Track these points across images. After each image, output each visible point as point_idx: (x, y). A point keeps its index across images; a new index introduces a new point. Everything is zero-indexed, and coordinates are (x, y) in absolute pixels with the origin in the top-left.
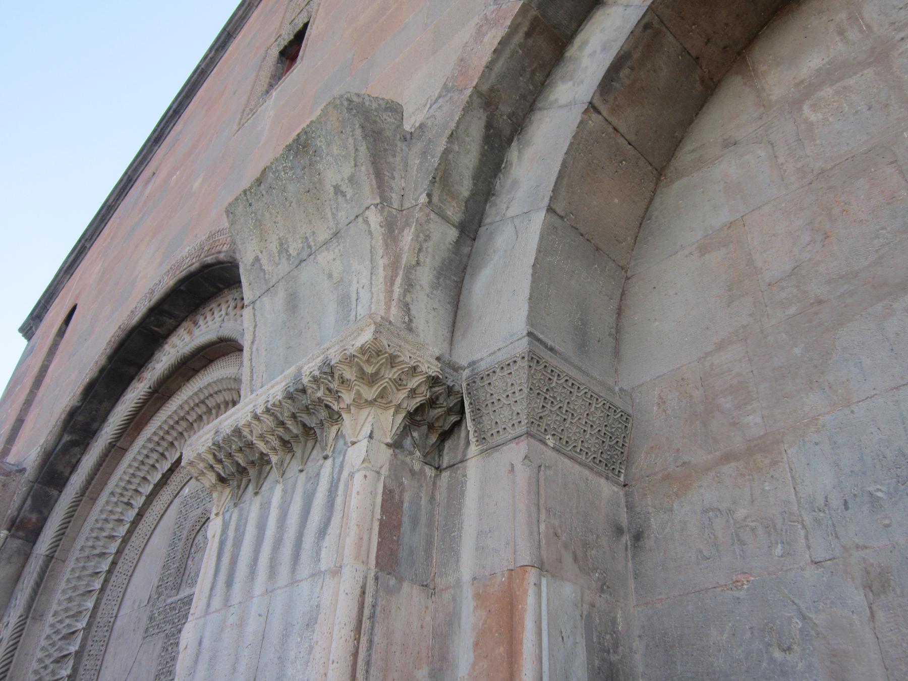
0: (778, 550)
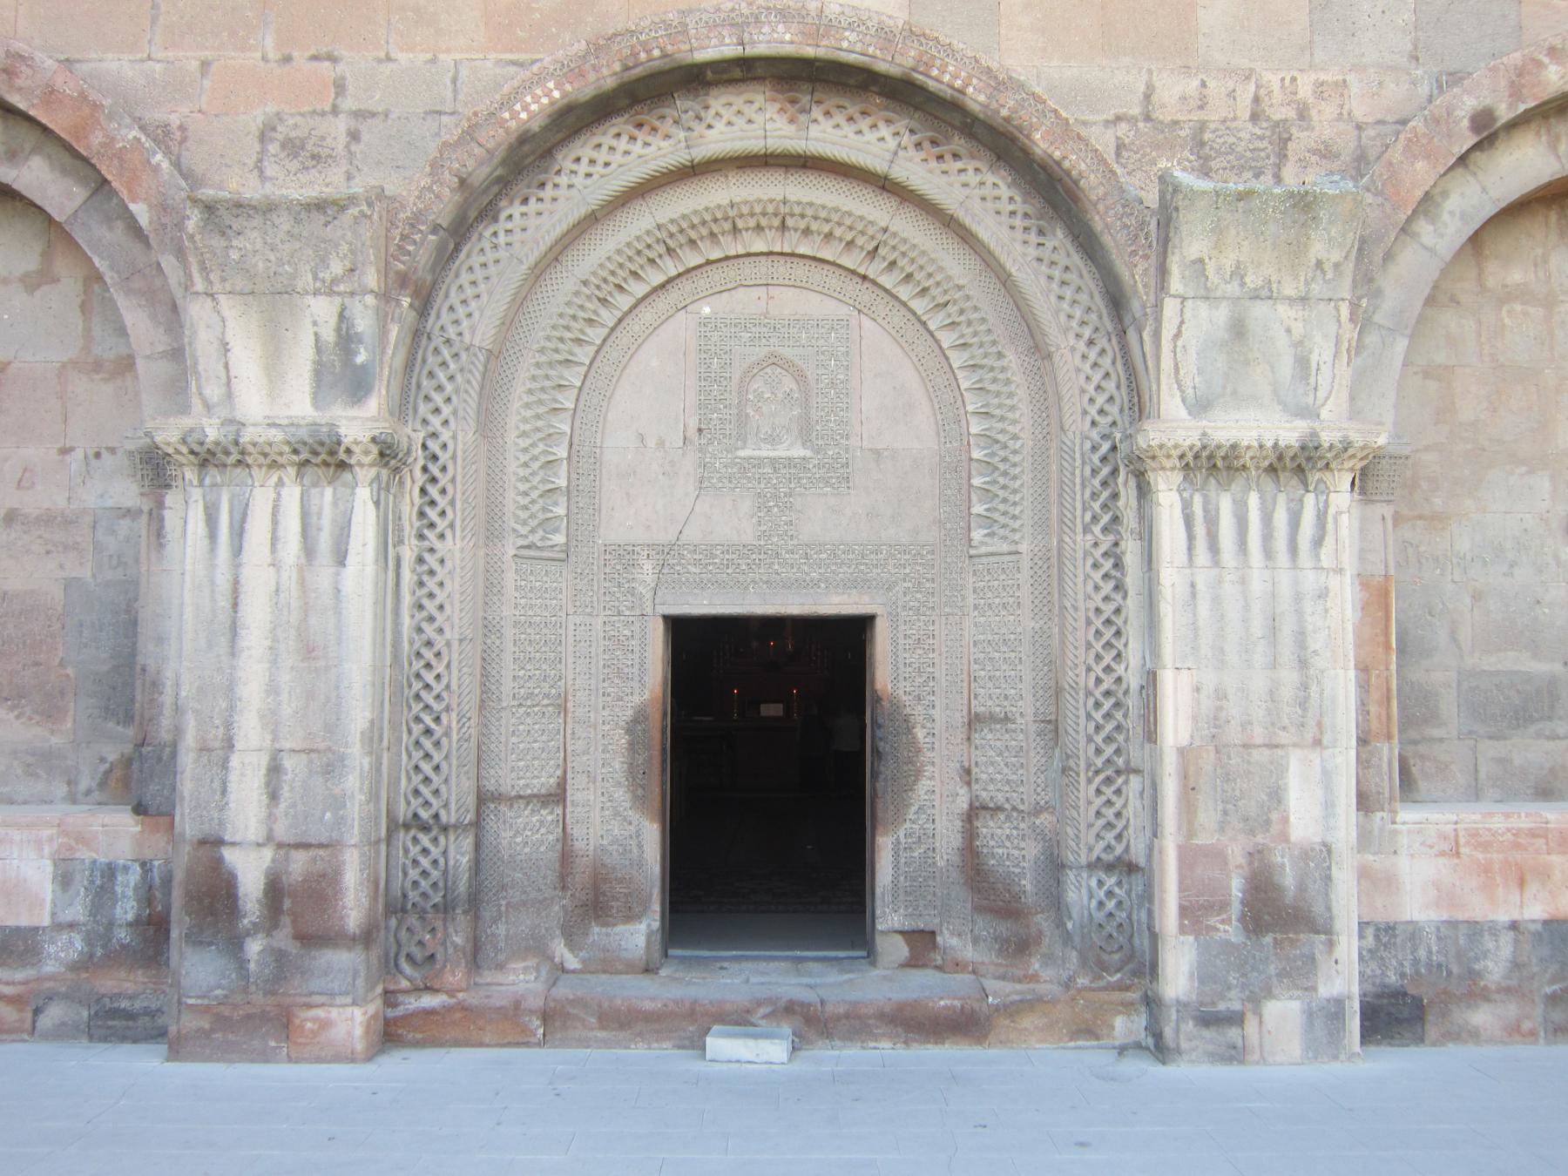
0: (1438, 571)
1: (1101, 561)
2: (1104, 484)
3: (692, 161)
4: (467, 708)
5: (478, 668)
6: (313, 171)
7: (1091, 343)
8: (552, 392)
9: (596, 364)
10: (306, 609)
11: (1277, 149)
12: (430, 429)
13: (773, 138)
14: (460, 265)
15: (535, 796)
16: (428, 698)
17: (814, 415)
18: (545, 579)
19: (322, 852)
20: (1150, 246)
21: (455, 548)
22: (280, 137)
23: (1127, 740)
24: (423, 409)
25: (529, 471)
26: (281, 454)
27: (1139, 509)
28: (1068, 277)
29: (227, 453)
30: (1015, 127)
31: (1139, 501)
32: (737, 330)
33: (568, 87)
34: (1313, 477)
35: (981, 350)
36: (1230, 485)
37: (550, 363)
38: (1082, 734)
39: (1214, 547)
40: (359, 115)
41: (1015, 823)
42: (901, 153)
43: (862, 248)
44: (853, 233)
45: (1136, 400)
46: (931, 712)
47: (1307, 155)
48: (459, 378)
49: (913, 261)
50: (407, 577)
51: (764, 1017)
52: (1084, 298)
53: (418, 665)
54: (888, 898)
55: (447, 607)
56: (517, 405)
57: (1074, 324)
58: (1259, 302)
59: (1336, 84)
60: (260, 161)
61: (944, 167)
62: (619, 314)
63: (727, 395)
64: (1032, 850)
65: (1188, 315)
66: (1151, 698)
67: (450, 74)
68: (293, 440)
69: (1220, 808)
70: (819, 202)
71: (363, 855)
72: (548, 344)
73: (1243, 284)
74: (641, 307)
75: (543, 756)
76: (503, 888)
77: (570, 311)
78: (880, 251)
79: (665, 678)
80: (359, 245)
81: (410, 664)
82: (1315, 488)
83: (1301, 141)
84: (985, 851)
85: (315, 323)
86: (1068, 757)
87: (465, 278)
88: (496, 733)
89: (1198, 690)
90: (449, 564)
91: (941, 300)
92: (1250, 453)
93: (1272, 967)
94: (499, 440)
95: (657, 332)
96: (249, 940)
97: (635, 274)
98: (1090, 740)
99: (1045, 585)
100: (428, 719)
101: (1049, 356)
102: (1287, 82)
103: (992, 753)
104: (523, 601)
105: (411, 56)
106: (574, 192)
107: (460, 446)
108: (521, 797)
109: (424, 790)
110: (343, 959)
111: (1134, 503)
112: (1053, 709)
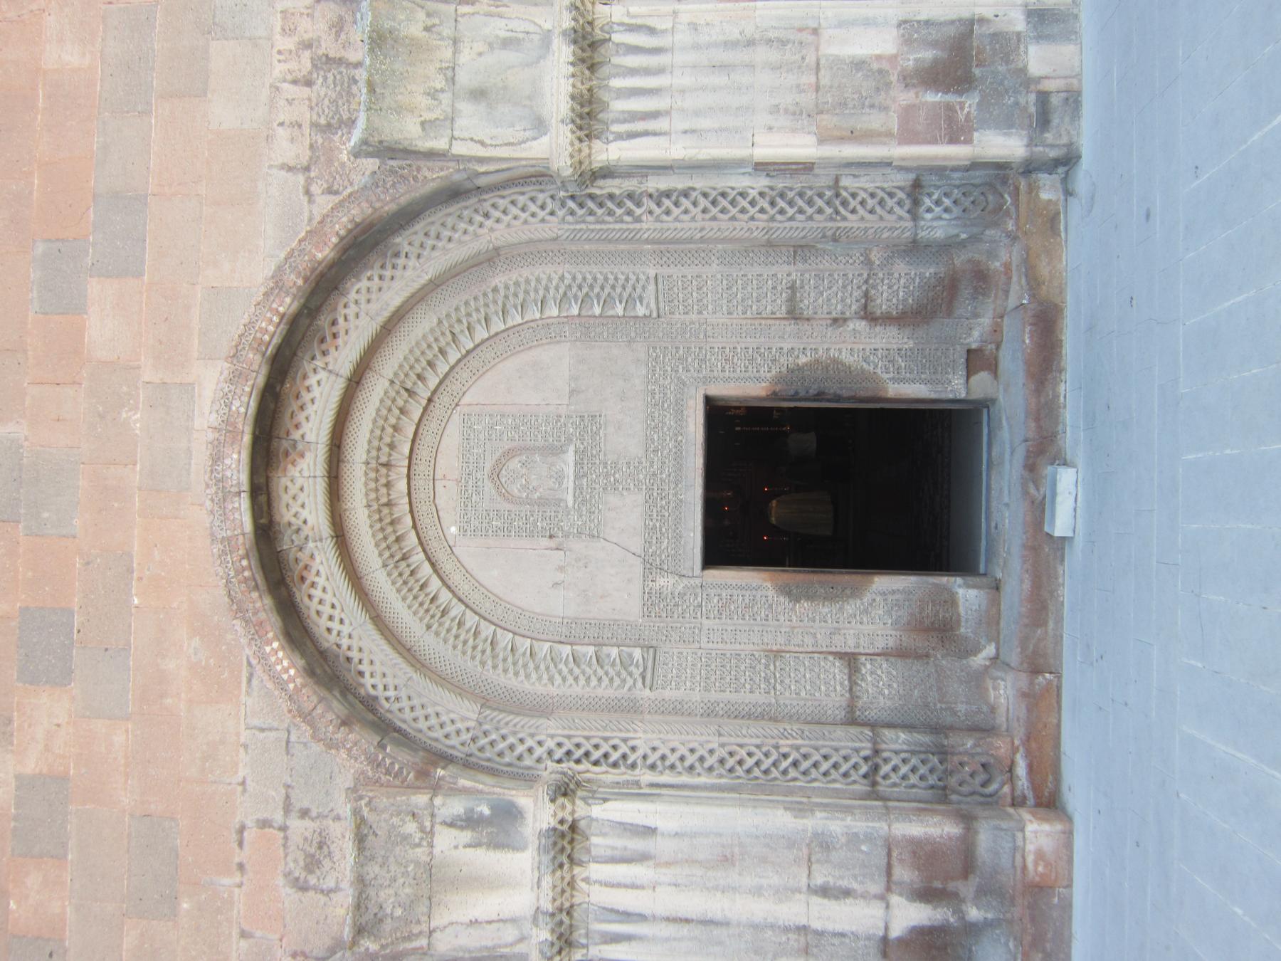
1: (664, 208)
2: (601, 205)
3: (333, 537)
4: (776, 731)
5: (741, 722)
6: (332, 848)
7: (487, 216)
8: (517, 656)
9: (494, 620)
10: (692, 862)
11: (334, 66)
12: (545, 756)
13: (315, 470)
14: (411, 728)
15: (850, 678)
16: (767, 763)
17: (540, 443)
18: (670, 665)
19: (895, 854)
20: (410, 166)
21: (644, 737)
22: (303, 875)
23: (811, 188)
24: (528, 762)
25: (581, 677)
26: (563, 878)
27: (622, 177)
28: (433, 234)
29: (561, 923)
30: (312, 272)
31: (616, 177)
32: (470, 505)
33: (270, 635)
34: (599, 34)
35: (491, 306)
36: (604, 102)
37: (493, 657)
38: (805, 224)
39: (655, 115)
40: (287, 809)
41: (878, 281)
42: (330, 367)
43: (406, 402)
44: (394, 409)
45: (534, 179)
46: (785, 350)
47: (340, 41)
48: (504, 731)
49: (417, 360)
50: (667, 778)
51: (1038, 490)
52: (450, 221)
53: (740, 771)
54: (940, 388)
55: (691, 745)
56: (527, 686)
57: (471, 229)
58: (456, 78)
59: (284, 19)
60: (322, 891)
61: (342, 333)
62: (455, 601)
63: (523, 514)
64: (900, 267)
65: (466, 135)
66: (776, 167)
67: (257, 733)
68: (551, 868)
69: (868, 110)
70: (368, 435)
71: (897, 820)
72: (478, 658)
73: (442, 91)
74: (450, 583)
75: (816, 670)
76: (927, 705)
77: (452, 639)
78: (409, 387)
79: (753, 570)
80: (393, 808)
81: (739, 777)
82: (608, 33)
83: (329, 46)
84: (901, 307)
85: (456, 847)
86: (824, 236)
87: (422, 725)
88: (797, 708)
89: (770, 128)
90: (656, 743)
91: (449, 337)
92: (579, 85)
93: (1000, 68)
94: (555, 700)
95: (469, 570)
96: (967, 918)
97: (422, 587)
98: (810, 218)
99: (682, 255)
100: (785, 764)
101: (497, 249)
102: (281, 57)
103: (820, 301)
104: (688, 684)
105: (241, 765)
106: (355, 634)
107: (560, 732)
108: (851, 689)
109: (844, 768)
110: (985, 838)
111: (617, 182)
112: (784, 249)
